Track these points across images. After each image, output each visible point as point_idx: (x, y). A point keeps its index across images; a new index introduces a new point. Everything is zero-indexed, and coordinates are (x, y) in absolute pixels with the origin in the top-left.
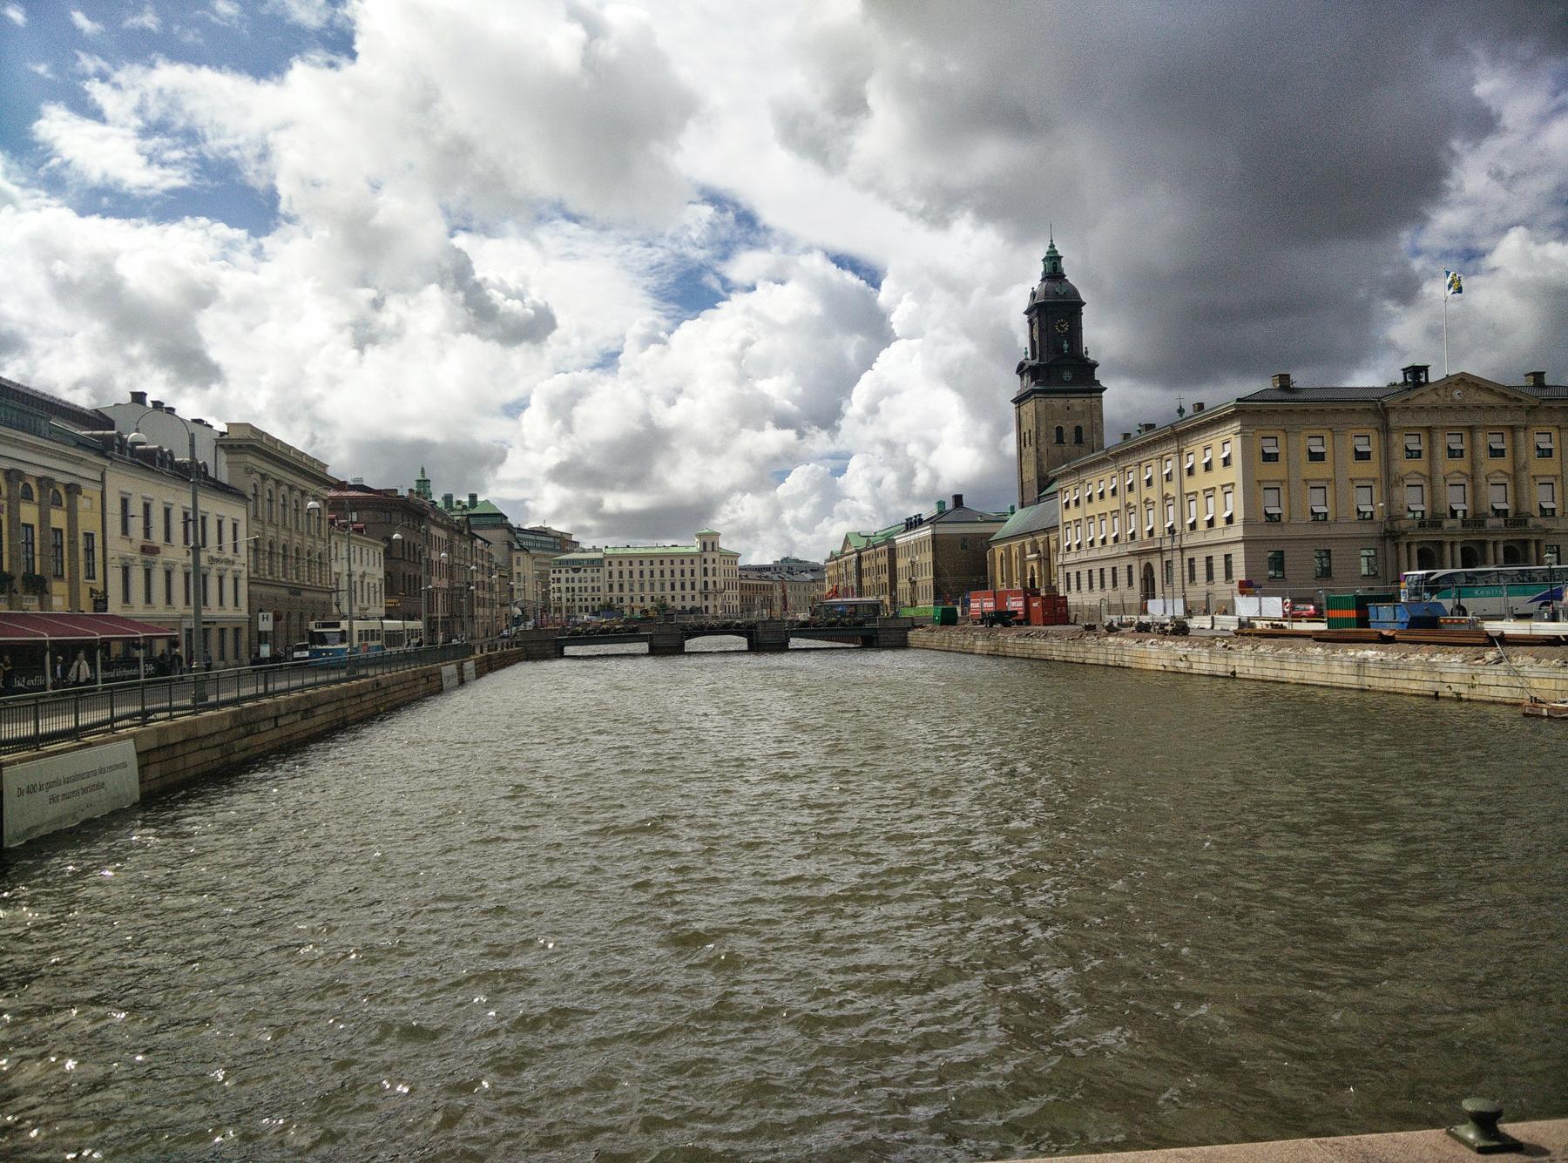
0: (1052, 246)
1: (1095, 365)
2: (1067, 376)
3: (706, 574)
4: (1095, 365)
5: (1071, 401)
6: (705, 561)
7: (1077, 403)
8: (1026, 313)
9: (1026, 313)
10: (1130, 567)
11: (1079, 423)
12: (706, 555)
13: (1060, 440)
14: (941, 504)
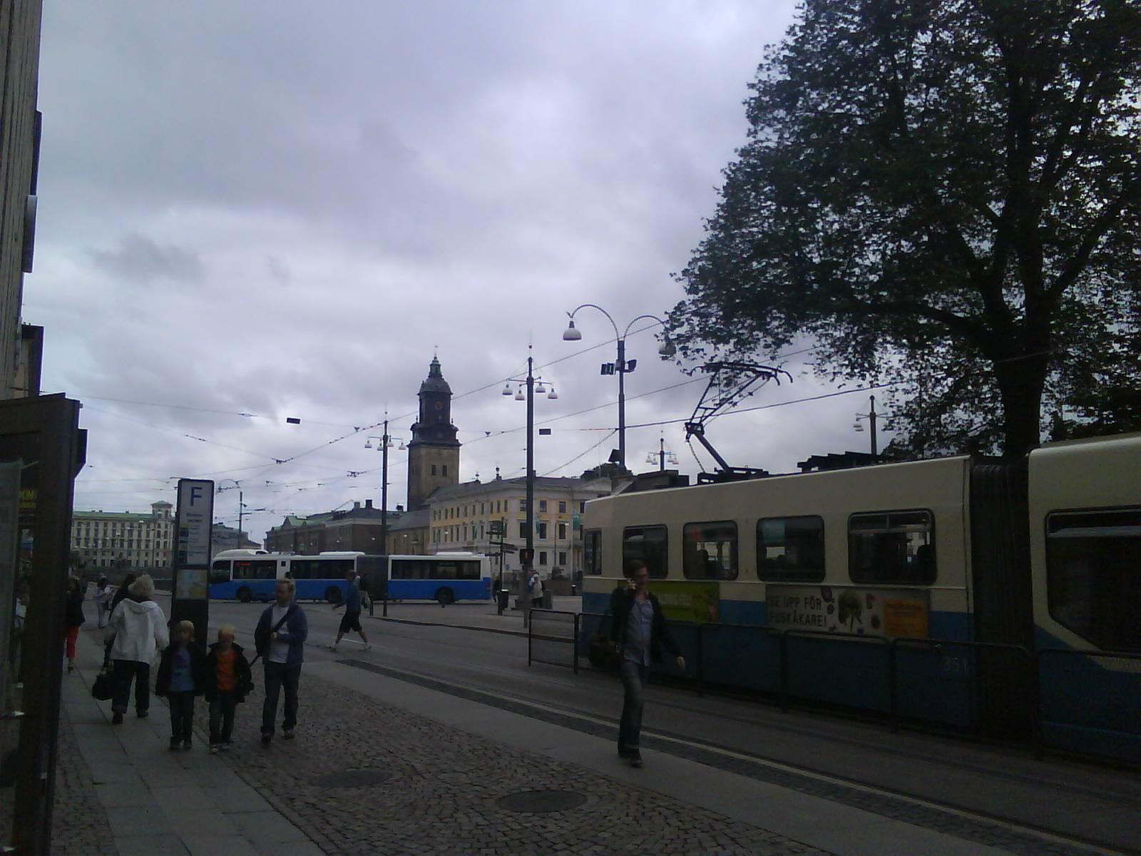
0: (435, 358)
1: (456, 430)
2: (440, 435)
3: (159, 536)
4: (456, 430)
5: (442, 451)
6: (159, 526)
7: (445, 452)
8: (418, 394)
9: (418, 394)
11: (446, 463)
13: (434, 473)
14: (357, 504)
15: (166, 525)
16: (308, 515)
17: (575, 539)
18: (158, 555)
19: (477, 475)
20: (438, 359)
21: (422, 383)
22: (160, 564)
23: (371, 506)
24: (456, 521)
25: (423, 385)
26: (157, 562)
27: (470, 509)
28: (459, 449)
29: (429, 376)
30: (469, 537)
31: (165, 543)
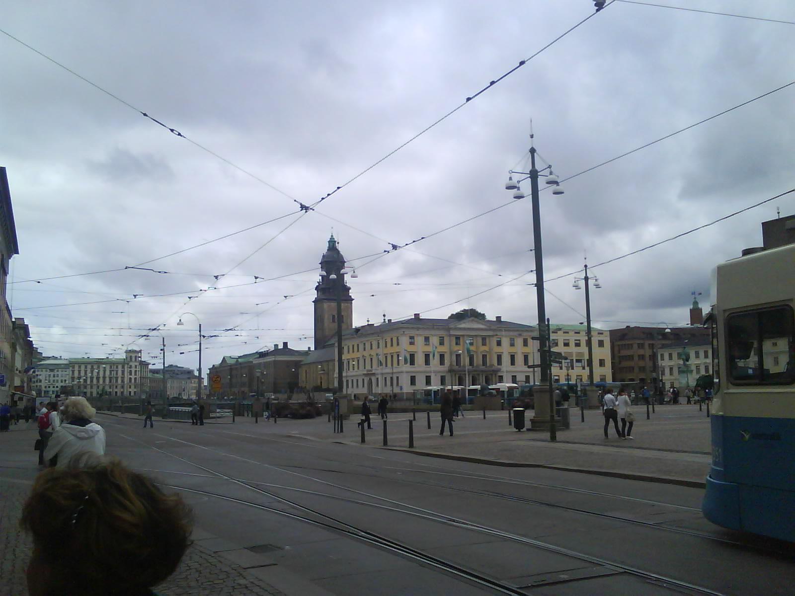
0: (332, 236)
1: (349, 289)
3: (131, 374)
4: (349, 289)
8: (320, 264)
9: (320, 264)
10: (363, 379)
12: (131, 364)
14: (276, 346)
15: (136, 366)
16: (239, 355)
17: (451, 365)
18: (130, 388)
19: (368, 321)
20: (334, 237)
21: (323, 255)
22: (132, 394)
23: (287, 346)
24: (358, 355)
25: (324, 256)
26: (130, 392)
27: (368, 346)
28: (352, 303)
29: (328, 250)
30: (368, 367)
31: (135, 379)
